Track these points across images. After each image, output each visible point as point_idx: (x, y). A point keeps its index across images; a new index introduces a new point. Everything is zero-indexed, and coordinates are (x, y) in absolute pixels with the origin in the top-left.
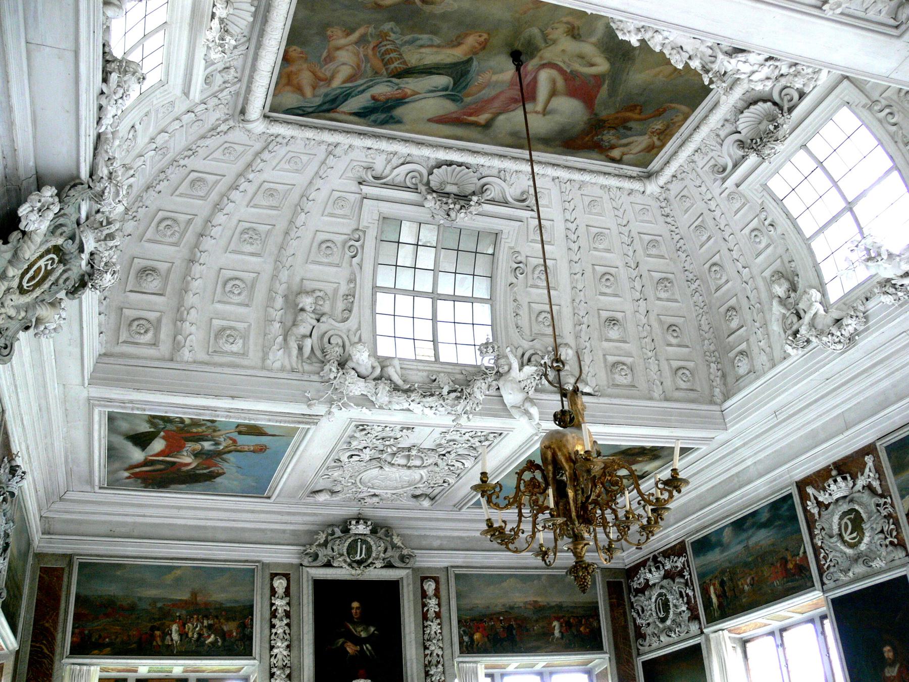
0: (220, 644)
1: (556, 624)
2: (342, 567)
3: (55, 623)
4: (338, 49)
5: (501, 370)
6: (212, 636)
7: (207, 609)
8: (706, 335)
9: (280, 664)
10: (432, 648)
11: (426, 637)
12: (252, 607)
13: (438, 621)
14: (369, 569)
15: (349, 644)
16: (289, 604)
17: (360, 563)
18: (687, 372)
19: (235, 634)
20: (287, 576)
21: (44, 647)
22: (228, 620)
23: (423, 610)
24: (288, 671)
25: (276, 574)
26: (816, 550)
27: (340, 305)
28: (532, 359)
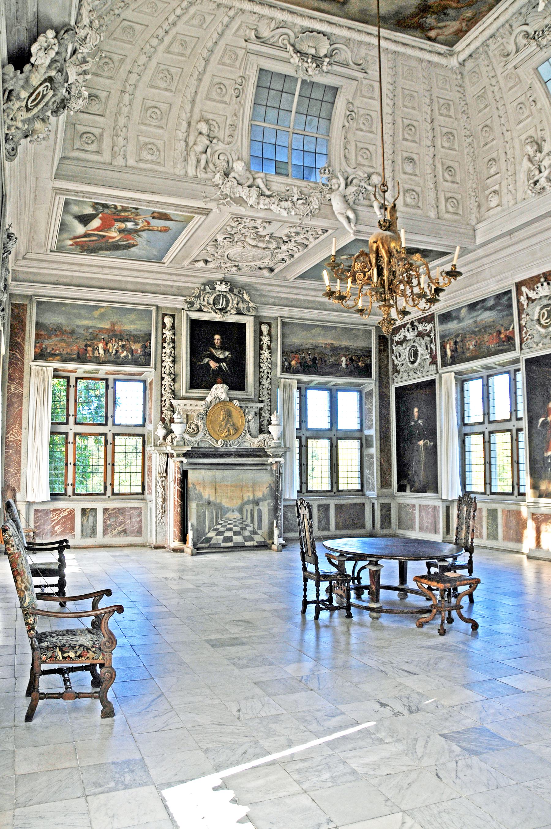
0: (130, 357)
1: (344, 359)
5: (333, 187)
6: (125, 352)
7: (121, 335)
8: (472, 177)
9: (167, 372)
11: (261, 360)
14: (227, 314)
15: (212, 362)
16: (174, 334)
17: (221, 310)
18: (455, 201)
20: (173, 316)
22: (135, 342)
24: (172, 376)
25: (166, 315)
26: (521, 328)
28: (354, 181)
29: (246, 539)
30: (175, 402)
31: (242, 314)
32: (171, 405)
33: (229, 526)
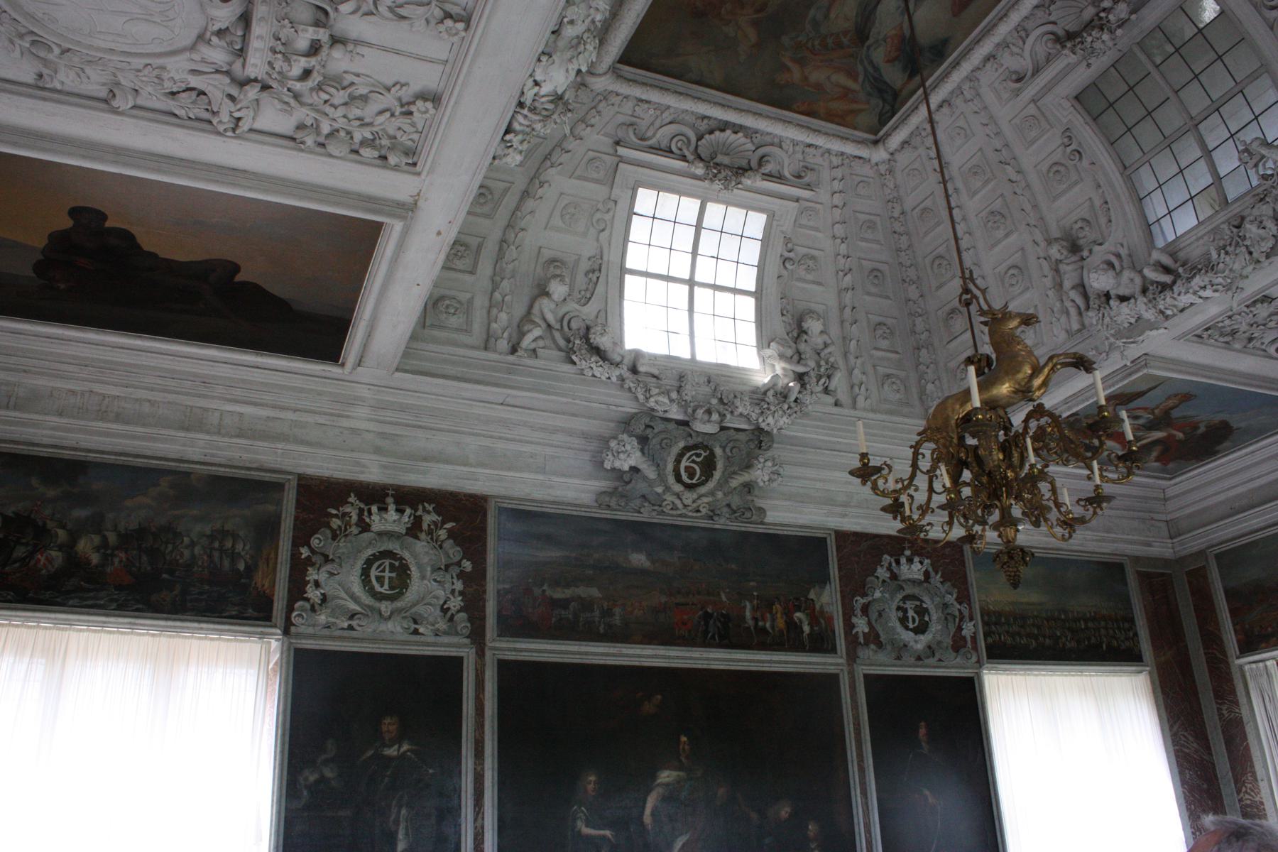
3: (1217, 623)
4: (806, 78)
21: (1216, 652)
27: (1103, 221)
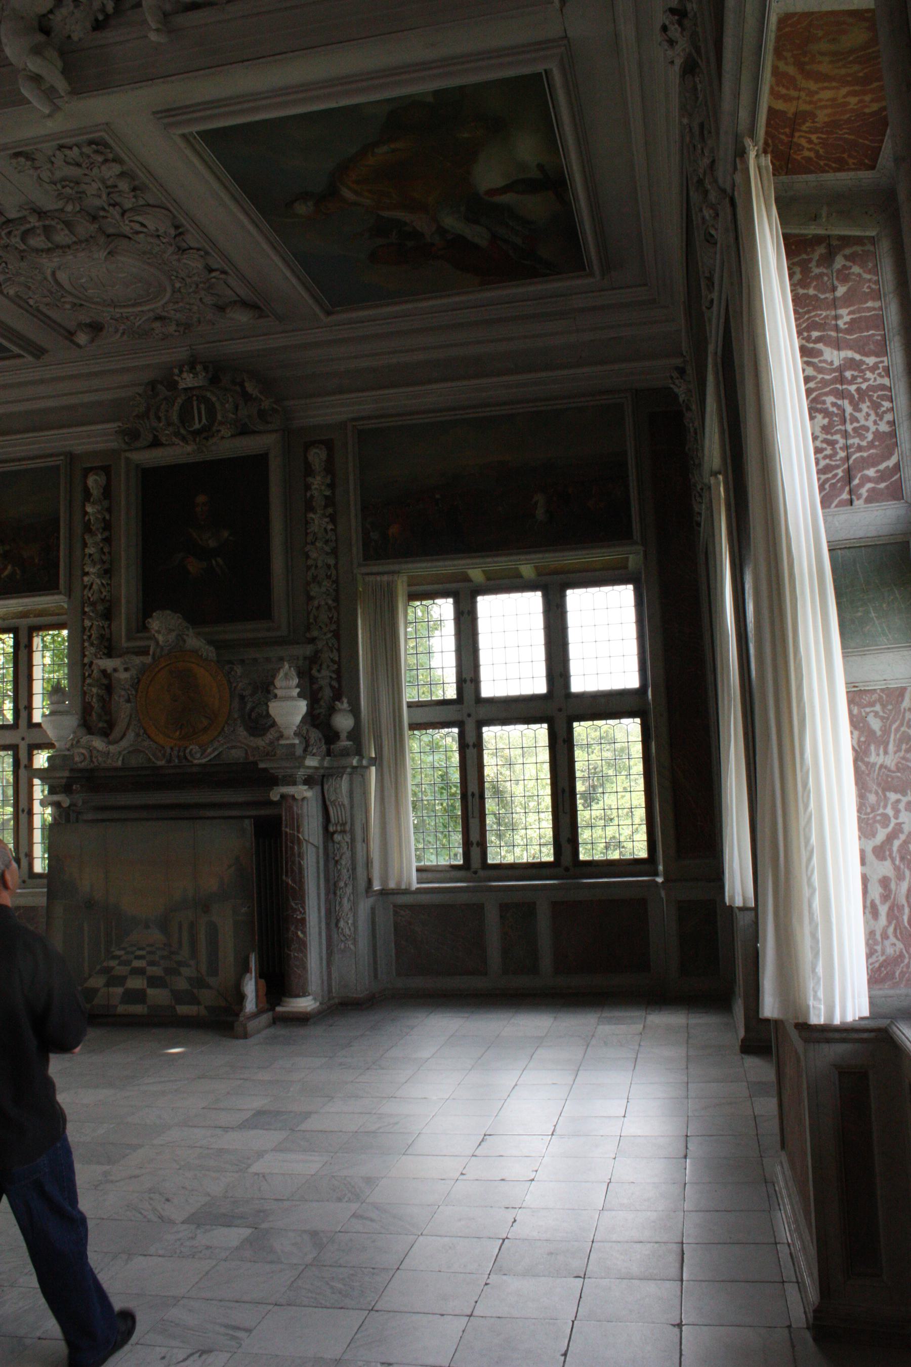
1: (540, 499)
2: (174, 444)
6: (9, 567)
10: (314, 555)
11: (310, 538)
12: (57, 520)
13: (330, 510)
16: (109, 510)
19: (36, 561)
20: (106, 470)
23: (306, 495)
24: (100, 607)
29: (179, 997)
30: (108, 664)
31: (254, 432)
32: (104, 672)
33: (137, 964)
